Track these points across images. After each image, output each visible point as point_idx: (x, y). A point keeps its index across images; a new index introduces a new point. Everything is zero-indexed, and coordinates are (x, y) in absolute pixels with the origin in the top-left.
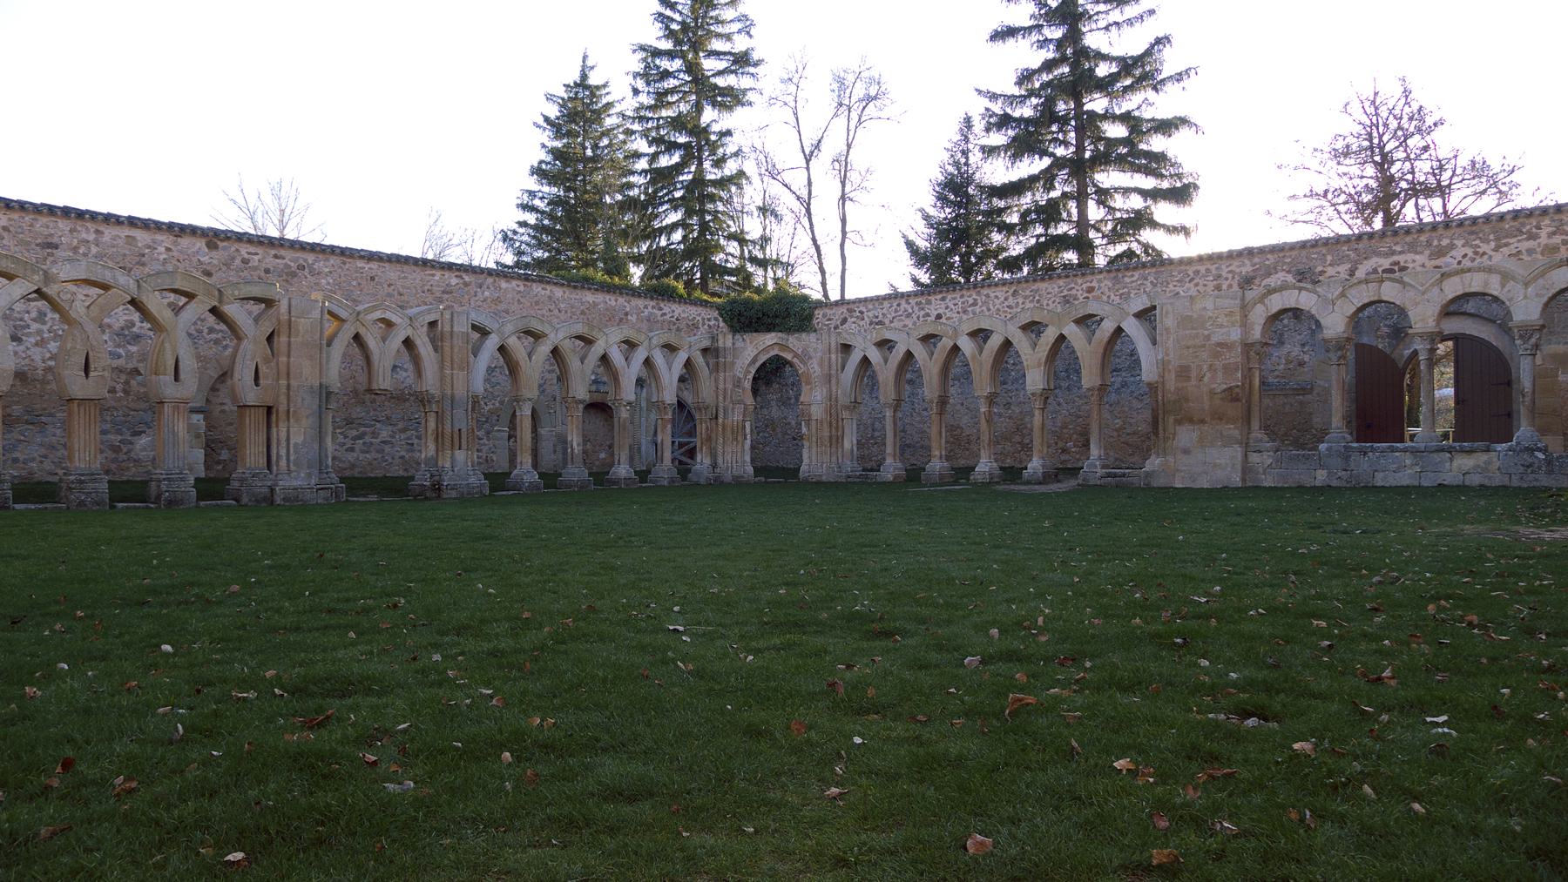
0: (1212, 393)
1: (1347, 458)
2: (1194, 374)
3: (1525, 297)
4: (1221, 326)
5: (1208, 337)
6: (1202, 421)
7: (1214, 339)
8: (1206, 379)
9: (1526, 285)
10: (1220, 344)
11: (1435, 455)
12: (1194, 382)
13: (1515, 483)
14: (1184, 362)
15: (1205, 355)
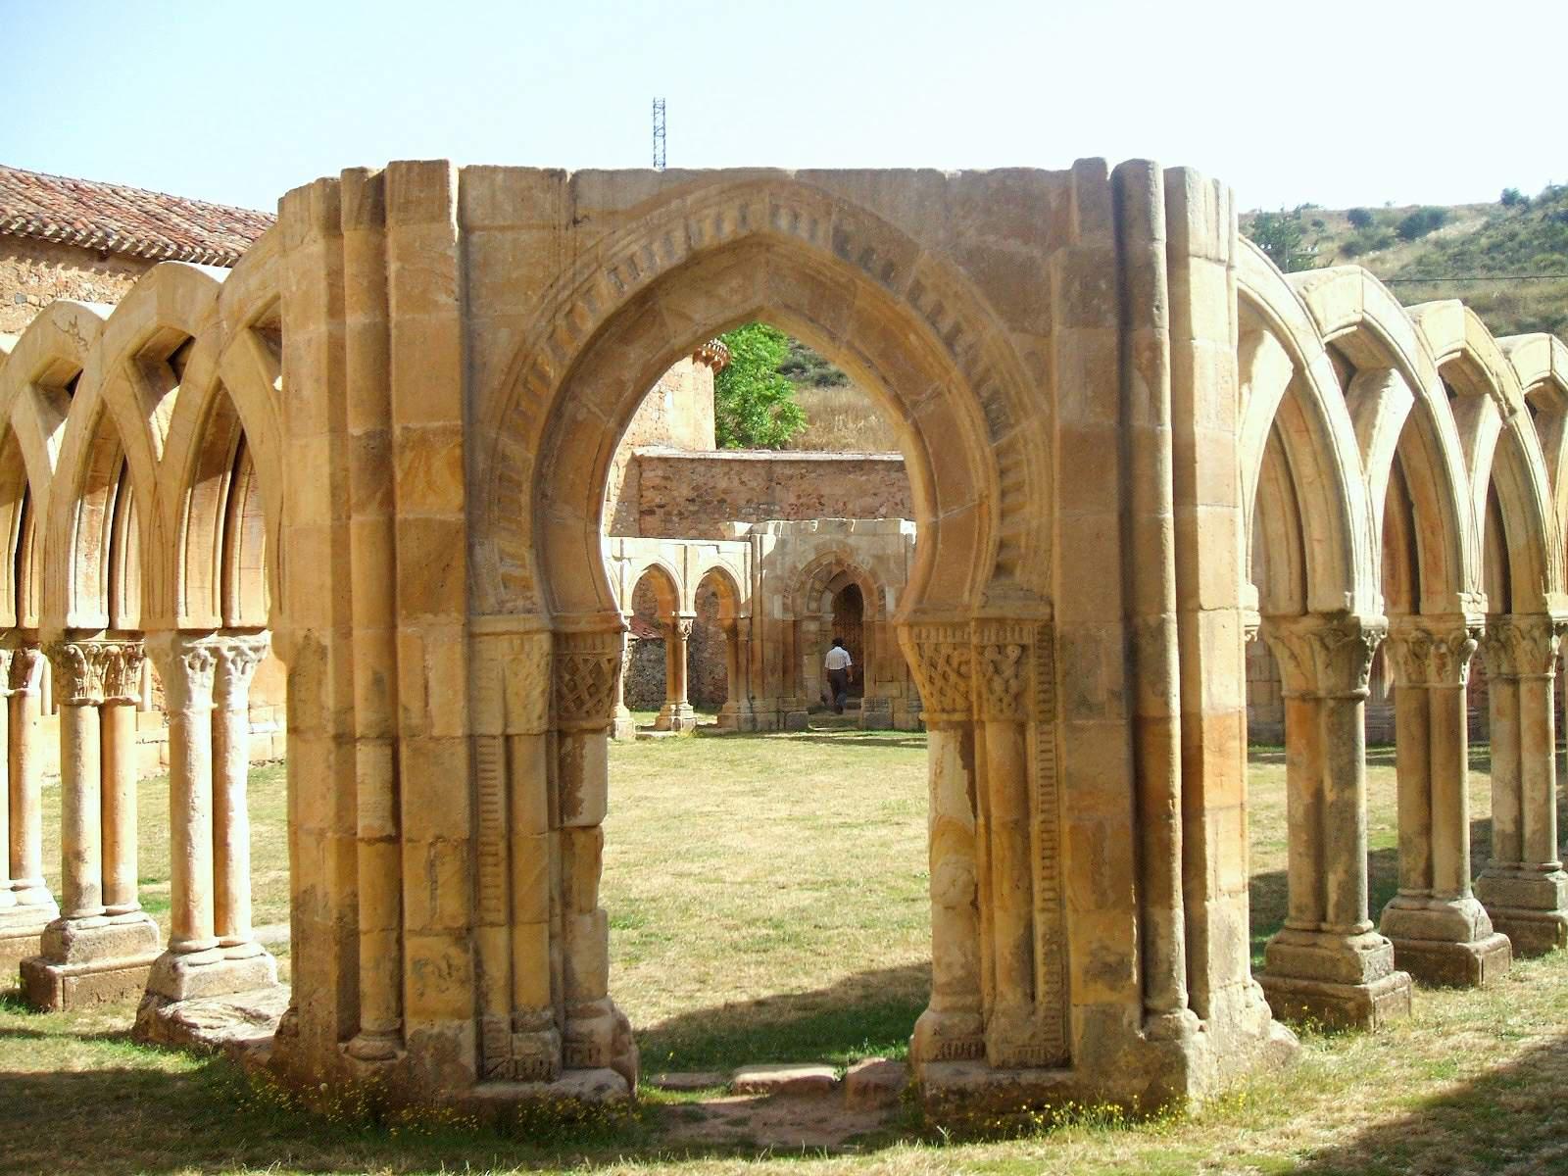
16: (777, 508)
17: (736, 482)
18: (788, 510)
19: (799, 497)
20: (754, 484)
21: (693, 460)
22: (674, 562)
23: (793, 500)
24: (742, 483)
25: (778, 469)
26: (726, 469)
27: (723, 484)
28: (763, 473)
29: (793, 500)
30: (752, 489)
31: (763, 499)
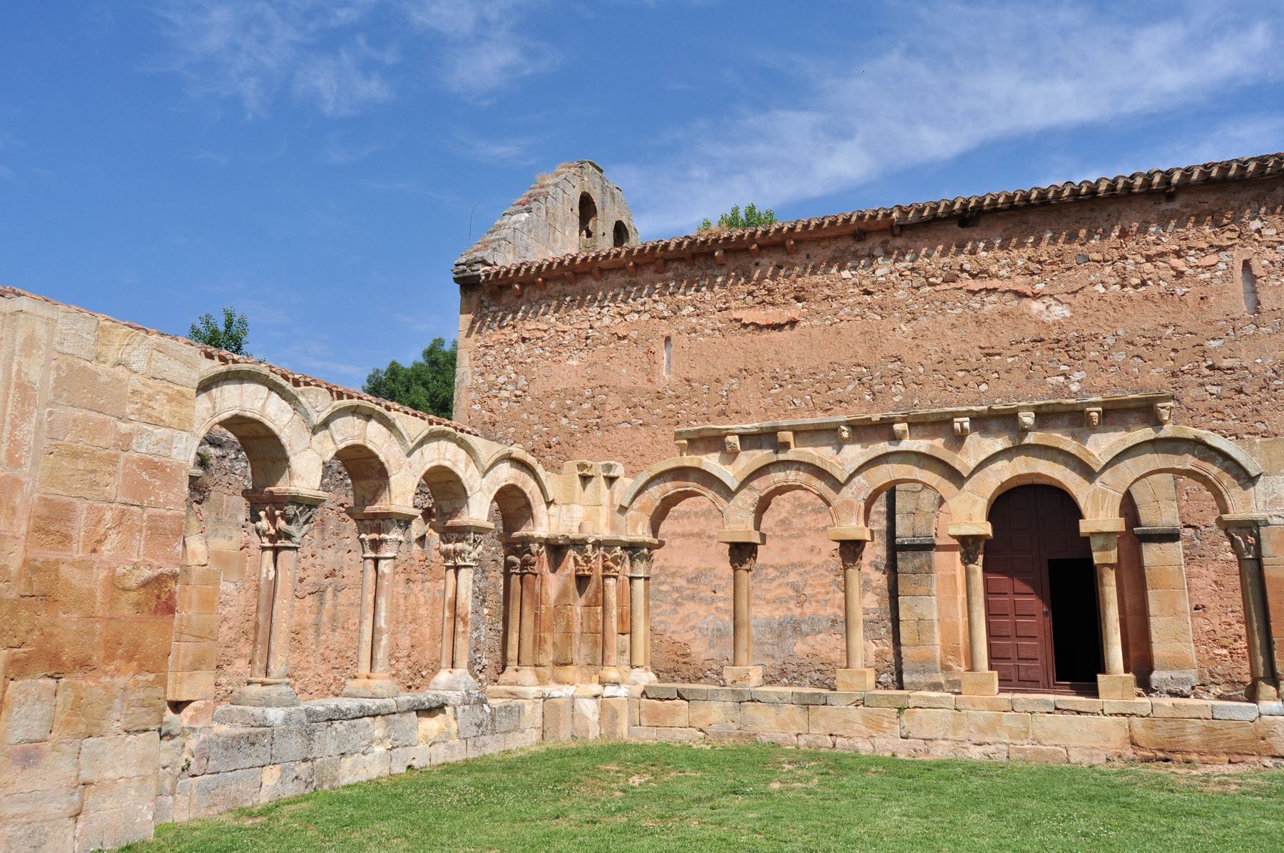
0: (115, 586)
1: (309, 735)
2: (80, 529)
3: (480, 490)
4: (158, 423)
5: (125, 442)
6: (84, 665)
7: (144, 447)
8: (106, 549)
9: (485, 474)
10: (152, 466)
11: (406, 718)
12: (77, 552)
13: (472, 755)
14: (59, 494)
15: (113, 486)
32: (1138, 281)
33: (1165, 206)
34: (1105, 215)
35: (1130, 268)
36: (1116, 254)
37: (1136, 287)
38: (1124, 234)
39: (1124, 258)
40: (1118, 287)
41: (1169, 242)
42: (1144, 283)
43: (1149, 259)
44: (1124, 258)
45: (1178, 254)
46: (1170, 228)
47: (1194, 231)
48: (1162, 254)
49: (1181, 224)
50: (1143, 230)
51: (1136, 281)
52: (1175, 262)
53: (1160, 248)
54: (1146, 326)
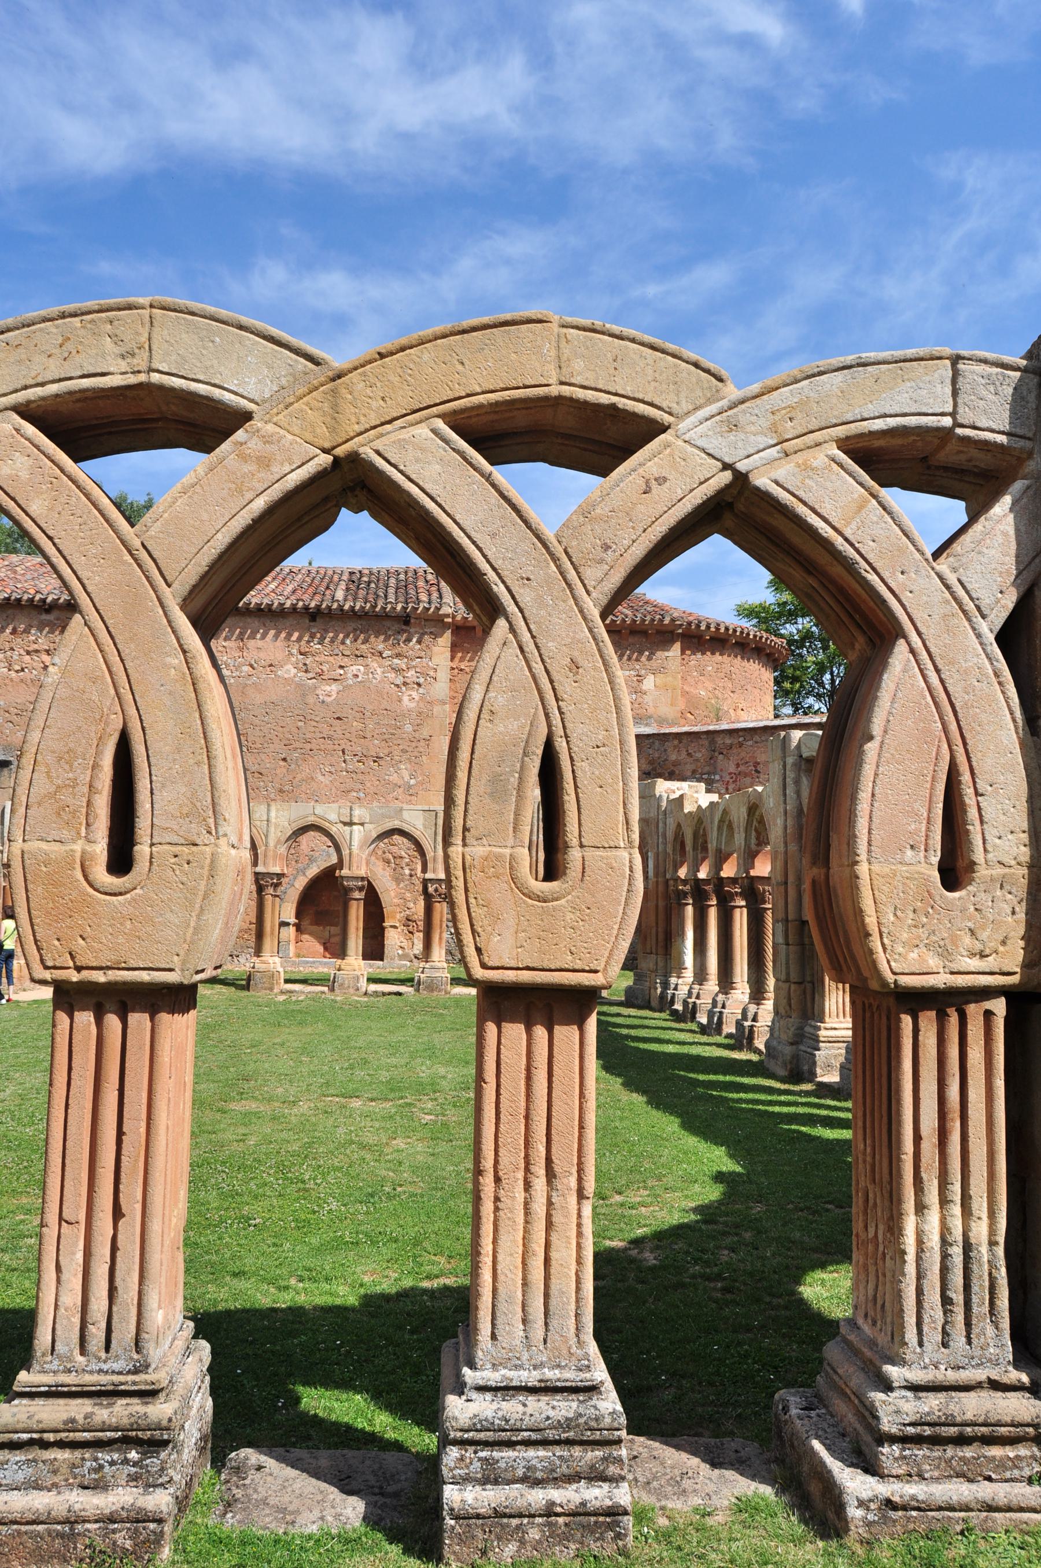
16: (717, 777)
17: (684, 754)
18: (727, 778)
19: (738, 765)
20: (699, 755)
21: (649, 735)
22: (421, 827)
23: (732, 768)
24: (689, 754)
25: (719, 741)
26: (676, 742)
27: (673, 757)
28: (706, 743)
29: (732, 768)
30: (697, 760)
31: (707, 769)
32: (19, 668)
33: (44, 617)
34: (5, 616)
35: (15, 657)
36: (7, 646)
37: (17, 671)
38: (14, 632)
39: (12, 649)
40: (6, 670)
41: (43, 643)
42: (23, 670)
43: (28, 653)
44: (12, 649)
45: (48, 652)
46: (45, 632)
47: (59, 637)
48: (37, 651)
49: (52, 632)
50: (27, 631)
51: (17, 668)
52: (46, 658)
53: (36, 647)
54: (19, 701)
